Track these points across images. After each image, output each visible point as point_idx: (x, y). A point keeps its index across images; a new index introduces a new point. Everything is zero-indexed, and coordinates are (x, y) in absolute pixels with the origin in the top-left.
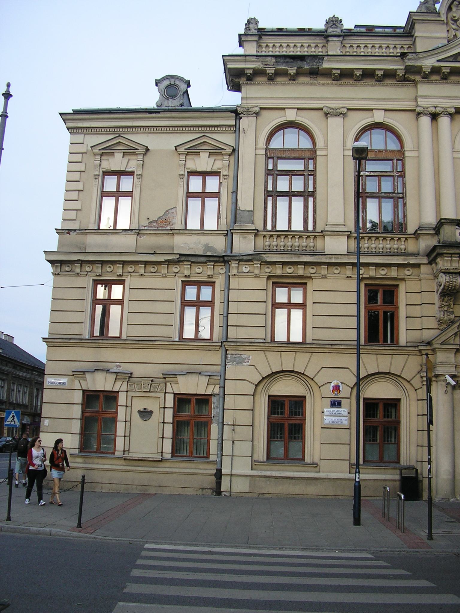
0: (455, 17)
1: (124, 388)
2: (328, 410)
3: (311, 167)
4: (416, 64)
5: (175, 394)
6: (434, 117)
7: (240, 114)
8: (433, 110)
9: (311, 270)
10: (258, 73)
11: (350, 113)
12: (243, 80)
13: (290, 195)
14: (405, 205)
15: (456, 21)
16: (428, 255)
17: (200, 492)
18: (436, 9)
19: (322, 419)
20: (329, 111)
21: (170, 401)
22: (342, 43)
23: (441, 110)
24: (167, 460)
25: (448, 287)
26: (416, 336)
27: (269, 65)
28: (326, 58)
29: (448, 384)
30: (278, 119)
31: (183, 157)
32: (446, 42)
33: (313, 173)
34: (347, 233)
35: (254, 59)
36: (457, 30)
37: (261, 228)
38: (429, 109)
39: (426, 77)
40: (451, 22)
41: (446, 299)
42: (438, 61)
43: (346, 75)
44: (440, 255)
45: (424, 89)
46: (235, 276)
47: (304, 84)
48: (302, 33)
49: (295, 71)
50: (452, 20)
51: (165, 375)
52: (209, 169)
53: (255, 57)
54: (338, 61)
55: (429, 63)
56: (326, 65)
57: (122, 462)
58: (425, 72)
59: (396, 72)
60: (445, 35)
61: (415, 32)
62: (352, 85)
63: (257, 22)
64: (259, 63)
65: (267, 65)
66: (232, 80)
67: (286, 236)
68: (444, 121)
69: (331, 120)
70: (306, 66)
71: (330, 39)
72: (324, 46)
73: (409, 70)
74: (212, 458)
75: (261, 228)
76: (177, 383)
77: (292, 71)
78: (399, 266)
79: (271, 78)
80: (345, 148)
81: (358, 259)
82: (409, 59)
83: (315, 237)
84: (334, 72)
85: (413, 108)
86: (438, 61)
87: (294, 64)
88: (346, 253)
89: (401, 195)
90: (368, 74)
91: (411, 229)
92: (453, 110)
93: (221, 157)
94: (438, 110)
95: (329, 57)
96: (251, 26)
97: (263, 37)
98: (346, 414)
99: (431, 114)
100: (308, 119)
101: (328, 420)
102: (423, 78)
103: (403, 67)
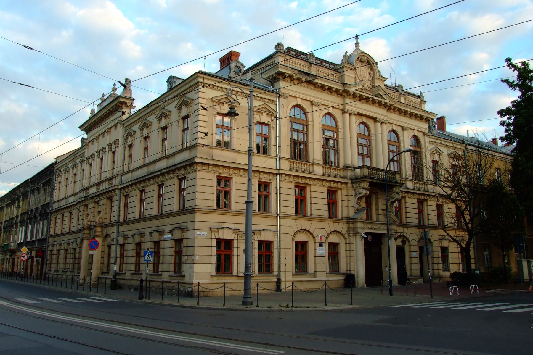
1: (236, 238)
2: (318, 248)
5: (259, 241)
6: (350, 114)
10: (290, 76)
17: (270, 292)
19: (315, 253)
26: (345, 215)
35: (291, 69)
44: (364, 181)
45: (347, 100)
46: (283, 181)
54: (322, 80)
55: (352, 90)
56: (317, 81)
57: (236, 278)
68: (353, 117)
71: (313, 65)
74: (276, 273)
78: (341, 183)
90: (330, 89)
91: (341, 166)
101: (318, 253)
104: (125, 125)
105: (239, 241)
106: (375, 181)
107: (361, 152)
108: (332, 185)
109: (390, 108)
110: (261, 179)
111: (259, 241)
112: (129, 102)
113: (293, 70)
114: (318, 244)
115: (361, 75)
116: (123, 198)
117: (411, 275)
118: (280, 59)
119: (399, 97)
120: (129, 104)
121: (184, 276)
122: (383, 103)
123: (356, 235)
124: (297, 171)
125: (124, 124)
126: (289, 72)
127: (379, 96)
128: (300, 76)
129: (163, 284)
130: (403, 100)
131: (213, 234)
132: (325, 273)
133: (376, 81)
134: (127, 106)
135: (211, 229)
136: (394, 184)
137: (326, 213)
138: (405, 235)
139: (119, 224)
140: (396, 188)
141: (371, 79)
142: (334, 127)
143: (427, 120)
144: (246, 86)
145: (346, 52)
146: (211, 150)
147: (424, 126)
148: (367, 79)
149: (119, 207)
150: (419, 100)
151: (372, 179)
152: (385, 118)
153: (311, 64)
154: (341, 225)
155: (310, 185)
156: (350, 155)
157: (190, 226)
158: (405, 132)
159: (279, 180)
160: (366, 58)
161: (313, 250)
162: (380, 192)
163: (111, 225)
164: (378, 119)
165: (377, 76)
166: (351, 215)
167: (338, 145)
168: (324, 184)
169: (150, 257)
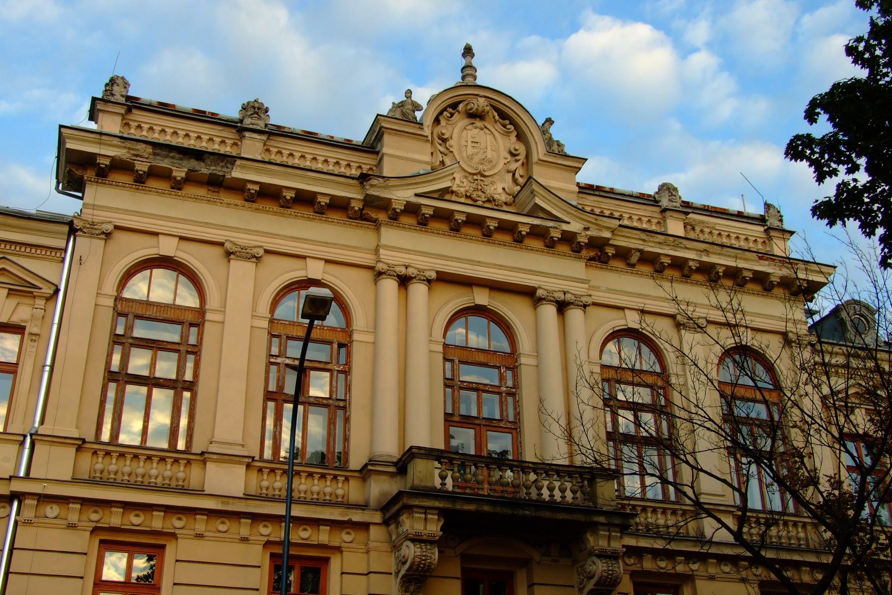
0: (443, 134)
3: (192, 340)
4: (383, 195)
6: (404, 281)
7: (77, 230)
8: (402, 271)
9: (176, 523)
10: (118, 166)
11: (268, 259)
12: (89, 174)
13: (151, 382)
14: (347, 420)
15: (444, 141)
16: (384, 509)
18: (415, 118)
20: (234, 249)
22: (265, 145)
23: (416, 272)
25: (419, 566)
27: (141, 156)
28: (238, 162)
30: (146, 249)
32: (429, 169)
33: (196, 351)
34: (247, 460)
35: (116, 141)
36: (446, 155)
37: (90, 437)
38: (397, 269)
39: (395, 217)
40: (437, 140)
41: (412, 588)
42: (416, 195)
43: (269, 195)
44: (409, 508)
45: (391, 236)
46: (28, 523)
47: (196, 198)
48: (199, 116)
49: (183, 175)
50: (439, 138)
53: (118, 140)
54: (258, 171)
55: (401, 196)
56: (237, 173)
58: (394, 209)
59: (349, 203)
60: (427, 158)
61: (382, 147)
62: (275, 213)
63: (126, 85)
64: (124, 151)
65: (137, 156)
66: (70, 171)
67: (136, 456)
68: (419, 290)
70: (204, 169)
71: (247, 134)
72: (235, 144)
73: (371, 202)
75: (90, 437)
77: (180, 173)
78: (334, 524)
79: (140, 180)
80: (254, 314)
81: (289, 509)
82: (372, 186)
83: (189, 462)
84: (250, 186)
85: (370, 263)
86: (416, 195)
87: (185, 163)
88: (241, 495)
89: (341, 404)
90: (305, 199)
91: (356, 462)
92: (434, 275)
93: (30, 301)
94: (411, 272)
95: (244, 162)
96: (115, 88)
97: (134, 111)
99: (399, 276)
100: (195, 258)
102: (390, 218)
103: (360, 197)
106: (472, 507)
113: (128, 144)
115: (470, 157)
119: (662, 222)
124: (92, 482)
127: (536, 211)
128: (165, 164)
130: (675, 227)
148: (501, 166)
150: (762, 229)
152: (577, 289)
159: (16, 522)
162: (537, 557)
164: (540, 293)
165: (539, 151)
167: (348, 388)
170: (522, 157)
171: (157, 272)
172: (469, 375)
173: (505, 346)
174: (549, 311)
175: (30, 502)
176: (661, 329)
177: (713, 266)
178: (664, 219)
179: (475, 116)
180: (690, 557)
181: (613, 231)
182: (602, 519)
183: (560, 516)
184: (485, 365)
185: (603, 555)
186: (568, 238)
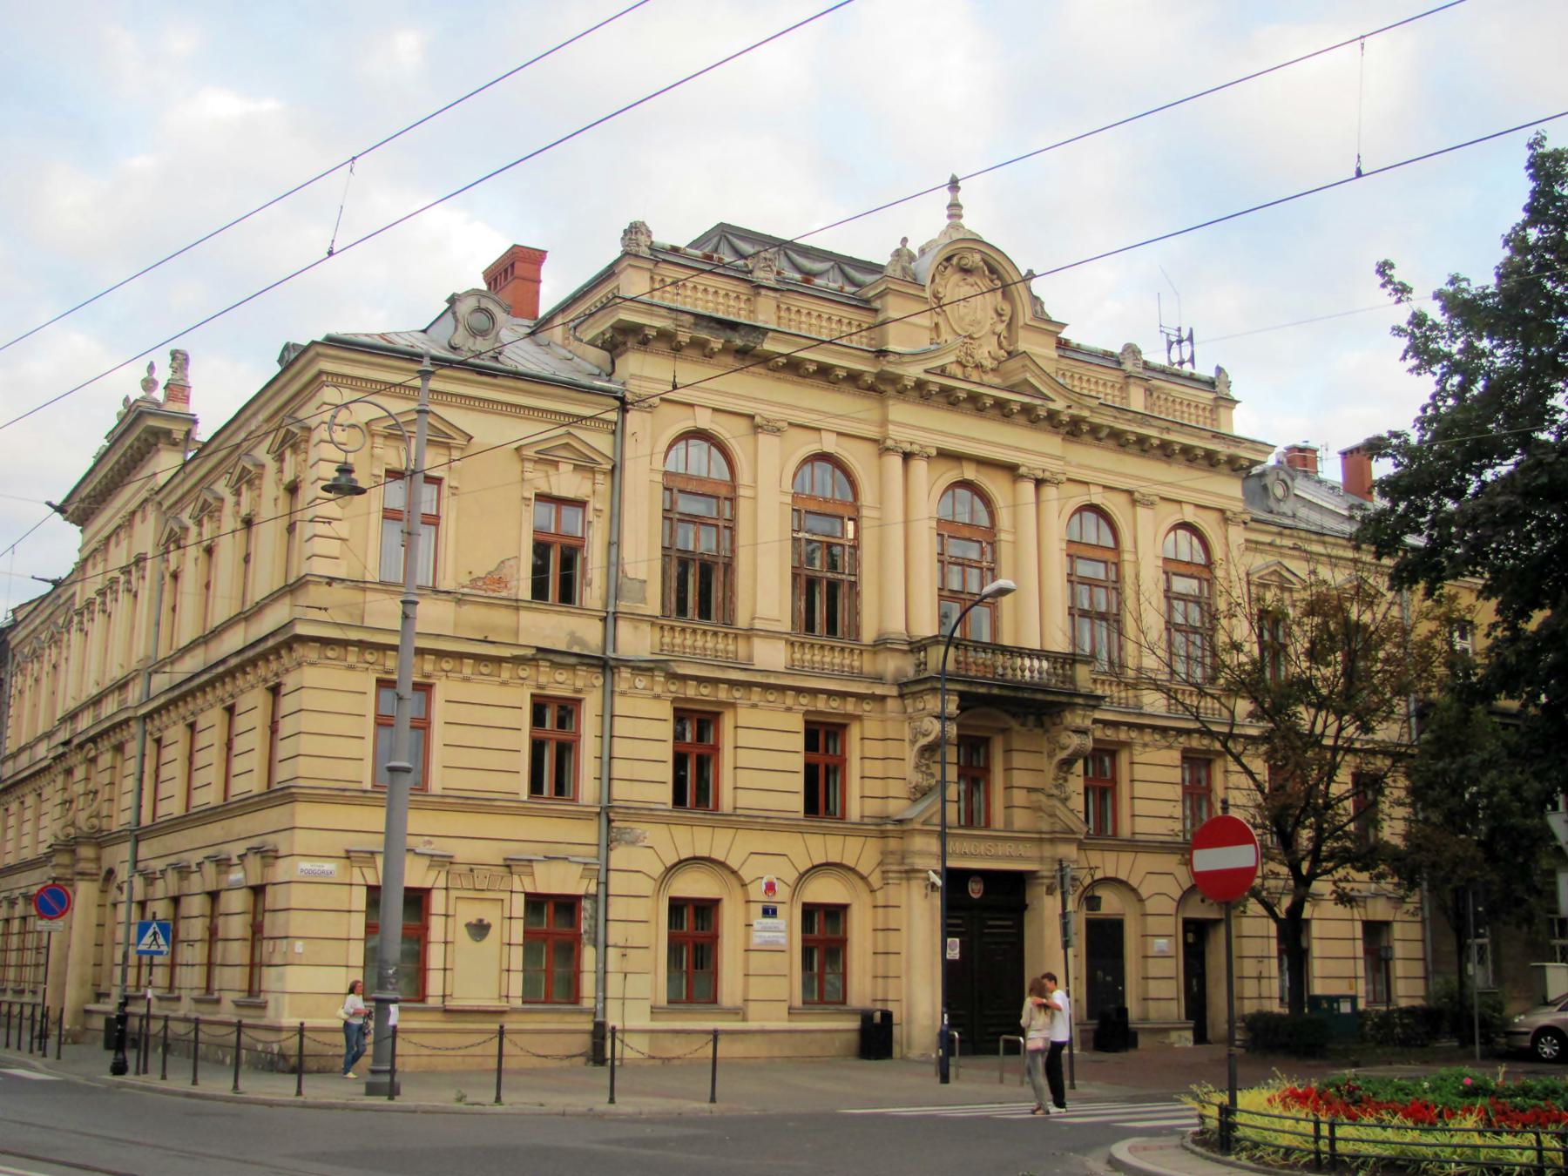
1: (442, 883)
2: (759, 922)
5: (527, 895)
6: (907, 457)
10: (664, 336)
19: (747, 937)
21: (519, 904)
24: (514, 1011)
26: (873, 807)
29: (933, 885)
31: (529, 466)
35: (663, 312)
39: (902, 392)
42: (927, 371)
43: (794, 367)
46: (623, 694)
51: (509, 865)
52: (571, 495)
55: (913, 372)
56: (769, 346)
57: (439, 1016)
62: (793, 382)
68: (919, 467)
69: (762, 437)
71: (763, 292)
73: (883, 377)
74: (588, 1003)
76: (532, 874)
78: (860, 697)
79: (676, 349)
86: (927, 371)
90: (824, 372)
92: (934, 452)
98: (783, 927)
101: (757, 939)
104: (166, 505)
105: (453, 894)
106: (982, 690)
107: (955, 584)
108: (821, 704)
109: (1074, 429)
110: (542, 688)
111: (527, 895)
112: (178, 431)
113: (674, 315)
114: (757, 909)
115: (962, 318)
116: (151, 747)
117: (1145, 1019)
118: (635, 283)
120: (179, 436)
121: (263, 1006)
122: (1043, 413)
123: (908, 879)
125: (160, 504)
126: (659, 323)
128: (704, 335)
129: (197, 1030)
131: (356, 871)
132: (785, 1006)
133: (1022, 334)
134: (175, 444)
135: (348, 855)
136: (1063, 699)
137: (797, 803)
138: (1099, 875)
139: (138, 834)
140: (1073, 711)
141: (1001, 328)
142: (844, 503)
143: (1235, 466)
144: (495, 376)
145: (905, 240)
146: (357, 596)
147: (1228, 490)
148: (987, 327)
149: (141, 780)
150: (1211, 396)
151: (971, 683)
152: (1054, 466)
153: (757, 287)
154: (854, 844)
155: (733, 705)
156: (900, 595)
157: (282, 843)
158: (1140, 510)
160: (977, 257)
161: (741, 929)
163: (115, 838)
164: (1023, 470)
165: (1025, 315)
166: (896, 808)
168: (789, 701)
169: (161, 941)
170: (1006, 318)
171: (692, 442)
172: (955, 549)
173: (984, 521)
174: (1028, 488)
175: (625, 673)
176: (1116, 506)
177: (1170, 443)
178: (1127, 384)
179: (966, 271)
180: (1131, 726)
181: (1091, 409)
182: (1080, 701)
183: (1050, 698)
184: (970, 540)
185: (1078, 731)
186: (1052, 416)
